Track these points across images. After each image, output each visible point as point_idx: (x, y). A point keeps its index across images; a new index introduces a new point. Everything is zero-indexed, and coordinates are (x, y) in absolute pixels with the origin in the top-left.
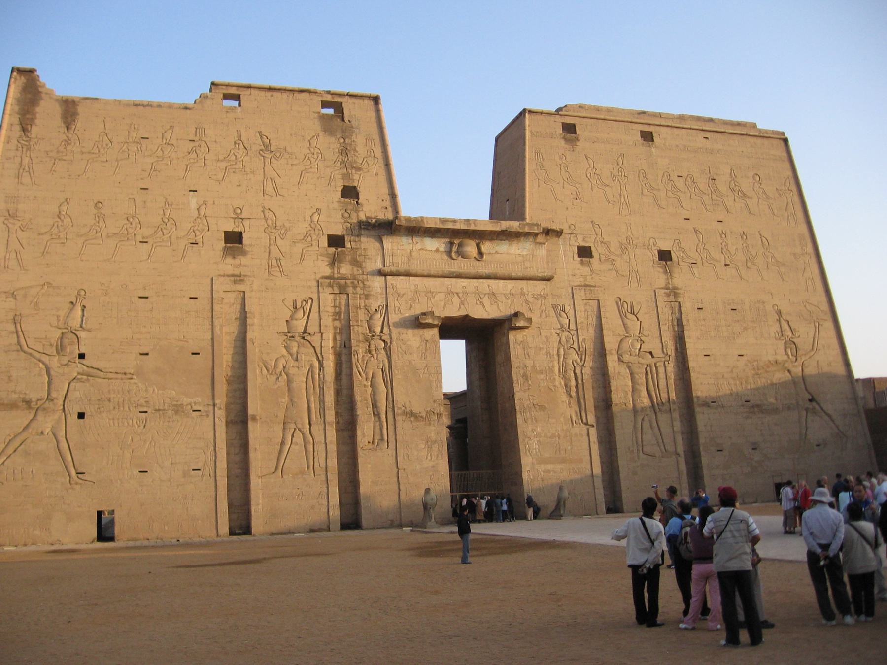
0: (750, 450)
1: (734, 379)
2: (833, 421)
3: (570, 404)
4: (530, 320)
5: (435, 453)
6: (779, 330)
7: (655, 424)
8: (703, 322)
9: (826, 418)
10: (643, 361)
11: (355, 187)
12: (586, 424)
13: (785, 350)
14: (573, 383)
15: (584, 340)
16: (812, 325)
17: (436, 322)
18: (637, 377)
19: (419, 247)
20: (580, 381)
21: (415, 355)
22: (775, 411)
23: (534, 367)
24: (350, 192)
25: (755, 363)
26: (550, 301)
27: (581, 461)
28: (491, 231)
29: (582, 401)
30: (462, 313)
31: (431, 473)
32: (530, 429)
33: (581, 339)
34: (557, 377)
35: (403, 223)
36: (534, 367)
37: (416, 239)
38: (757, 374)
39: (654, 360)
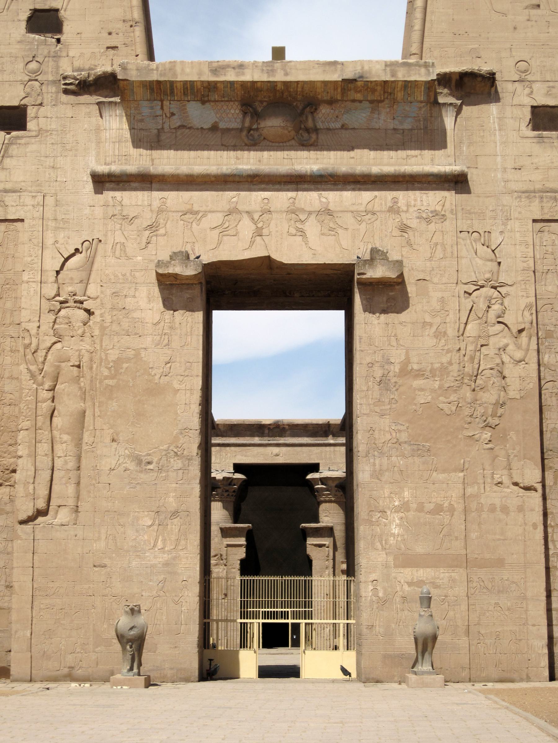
4: (399, 263)
5: (173, 538)
11: (57, 10)
17: (190, 271)
19: (176, 122)
20: (512, 394)
21: (148, 341)
23: (407, 361)
24: (45, 22)
27: (500, 563)
28: (325, 83)
30: (257, 252)
31: (161, 577)
32: (387, 492)
35: (133, 76)
36: (407, 361)
37: (170, 106)
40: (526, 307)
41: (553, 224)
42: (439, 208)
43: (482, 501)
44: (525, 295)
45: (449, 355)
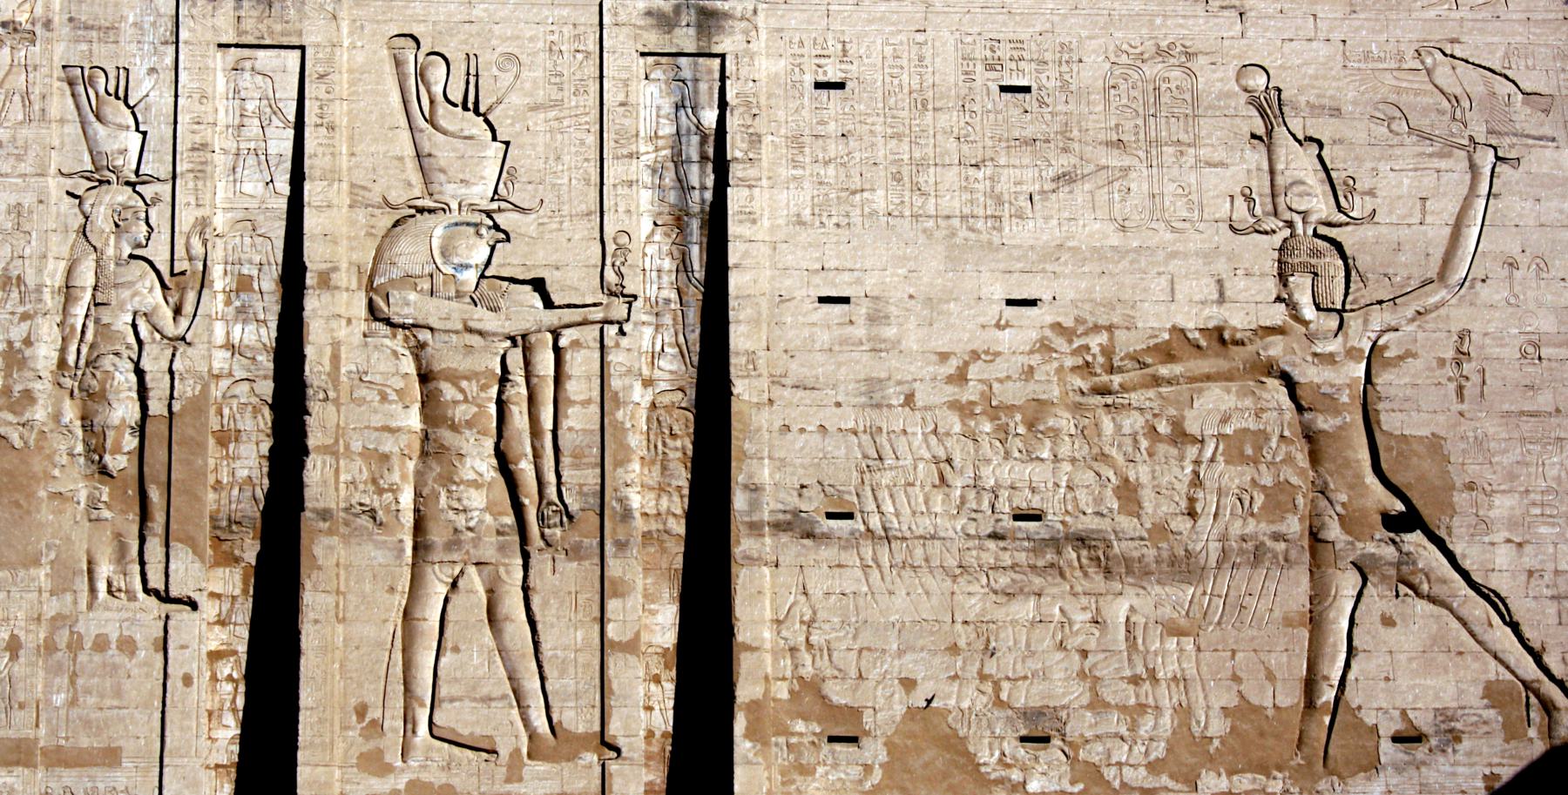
0: (1011, 746)
1: (964, 410)
2: (1515, 627)
3: (93, 504)
6: (1261, 185)
7: (513, 604)
8: (834, 148)
9: (1478, 609)
10: (483, 318)
12: (165, 597)
13: (1283, 278)
14: (124, 410)
15: (203, 224)
16: (1459, 162)
18: (449, 392)
20: (157, 407)
22: (1184, 567)
25: (1096, 342)
26: (61, 51)
29: (155, 495)
33: (186, 219)
34: (43, 388)
38: (1103, 391)
39: (552, 318)
40: (194, 226)
41: (261, 53)
42: (22, 18)
43: (80, 627)
44: (193, 202)
45: (25, 326)
